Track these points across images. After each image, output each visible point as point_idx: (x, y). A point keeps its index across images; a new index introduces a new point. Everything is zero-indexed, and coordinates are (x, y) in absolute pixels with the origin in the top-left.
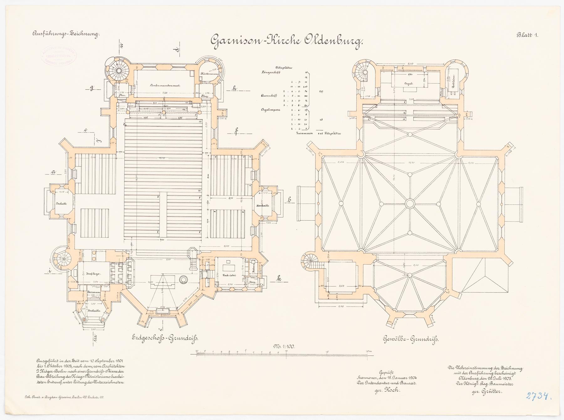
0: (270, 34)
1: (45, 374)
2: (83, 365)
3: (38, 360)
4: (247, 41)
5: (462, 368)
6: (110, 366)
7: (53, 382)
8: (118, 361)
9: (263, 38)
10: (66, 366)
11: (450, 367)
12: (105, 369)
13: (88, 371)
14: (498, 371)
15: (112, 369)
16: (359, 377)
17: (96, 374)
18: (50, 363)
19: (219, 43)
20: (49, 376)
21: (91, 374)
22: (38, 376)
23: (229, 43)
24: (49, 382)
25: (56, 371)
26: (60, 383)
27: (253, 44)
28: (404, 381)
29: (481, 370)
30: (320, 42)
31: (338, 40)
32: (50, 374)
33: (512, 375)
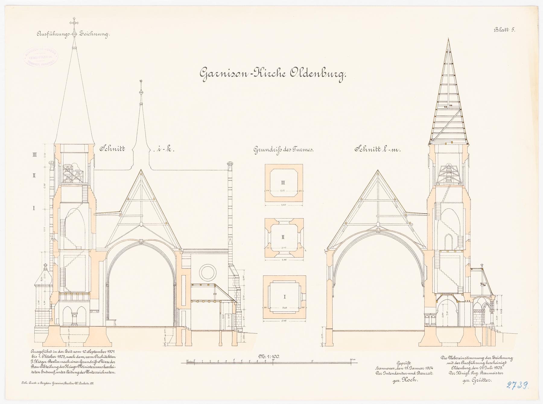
0: (258, 68)
1: (40, 365)
2: (76, 356)
3: (33, 351)
4: (234, 74)
5: (455, 358)
6: (102, 357)
7: (47, 372)
9: (249, 71)
11: (443, 358)
12: (98, 360)
13: (81, 362)
14: (489, 361)
16: (377, 368)
17: (89, 365)
18: (44, 354)
19: (208, 76)
21: (83, 364)
22: (33, 366)
23: (217, 76)
24: (42, 372)
25: (50, 361)
27: (240, 77)
28: (421, 371)
29: (472, 360)
30: (305, 75)
31: (322, 72)
32: (44, 364)
33: (503, 364)
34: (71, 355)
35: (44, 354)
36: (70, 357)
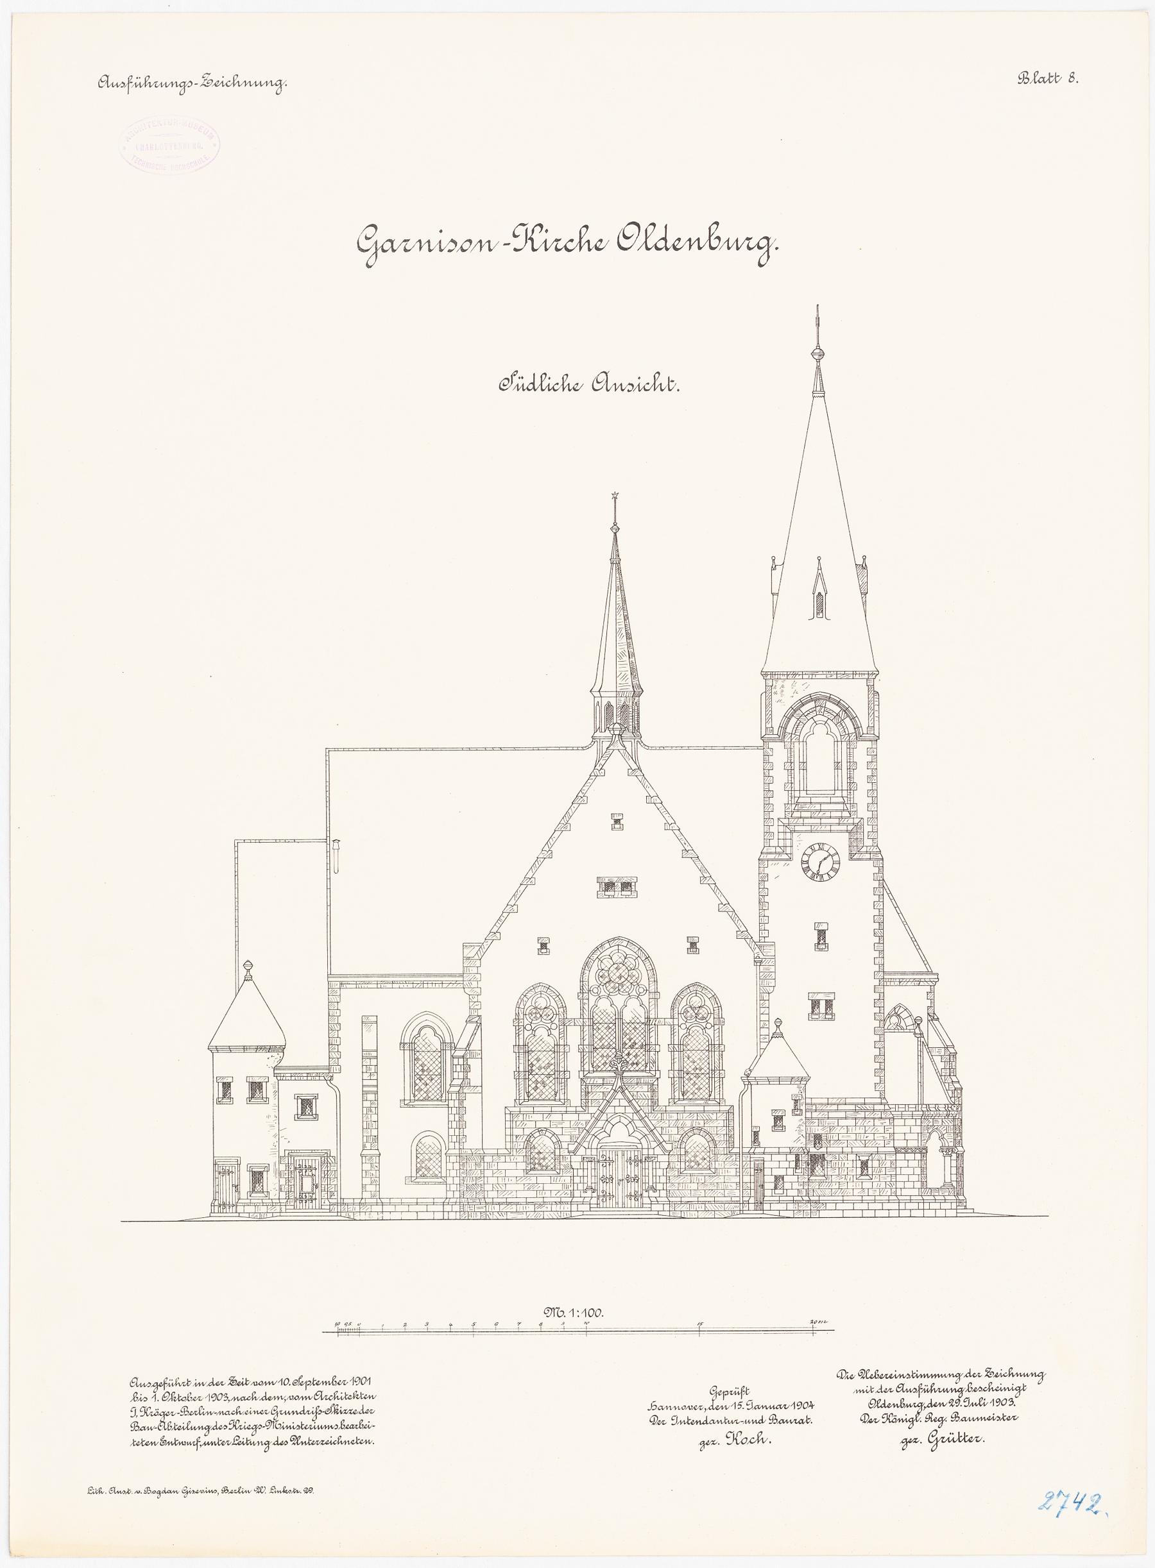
1: (155, 1421)
3: (135, 1382)
8: (360, 1381)
10: (215, 1397)
12: (325, 1405)
13: (276, 1412)
15: (344, 1405)
17: (297, 1420)
18: (171, 1390)
20: (166, 1427)
21: (282, 1419)
22: (135, 1427)
24: (164, 1442)
25: (185, 1411)
26: (196, 1444)
32: (167, 1419)
34: (246, 1391)
35: (171, 1390)
36: (244, 1399)
